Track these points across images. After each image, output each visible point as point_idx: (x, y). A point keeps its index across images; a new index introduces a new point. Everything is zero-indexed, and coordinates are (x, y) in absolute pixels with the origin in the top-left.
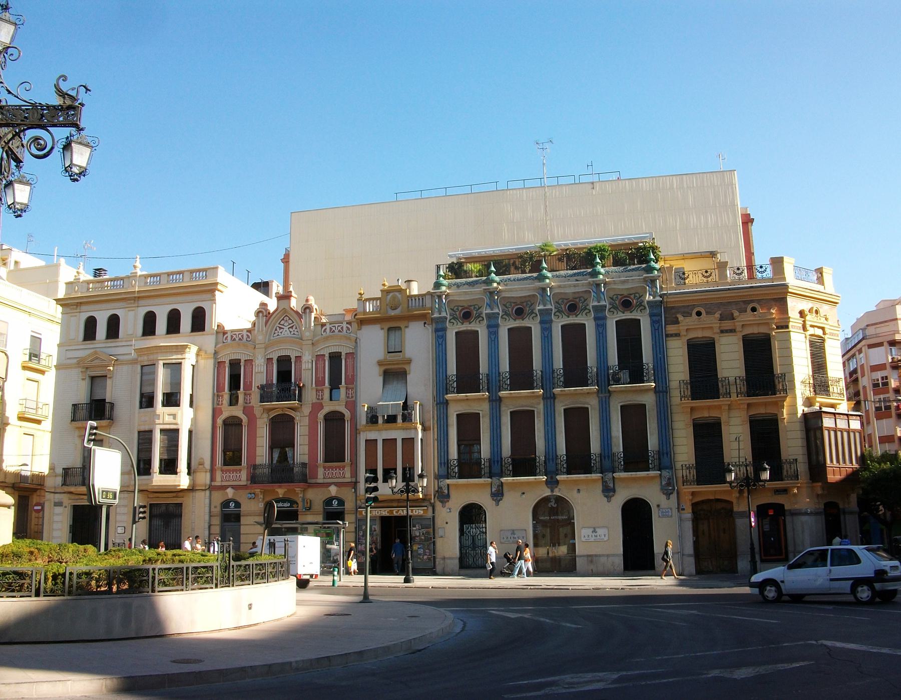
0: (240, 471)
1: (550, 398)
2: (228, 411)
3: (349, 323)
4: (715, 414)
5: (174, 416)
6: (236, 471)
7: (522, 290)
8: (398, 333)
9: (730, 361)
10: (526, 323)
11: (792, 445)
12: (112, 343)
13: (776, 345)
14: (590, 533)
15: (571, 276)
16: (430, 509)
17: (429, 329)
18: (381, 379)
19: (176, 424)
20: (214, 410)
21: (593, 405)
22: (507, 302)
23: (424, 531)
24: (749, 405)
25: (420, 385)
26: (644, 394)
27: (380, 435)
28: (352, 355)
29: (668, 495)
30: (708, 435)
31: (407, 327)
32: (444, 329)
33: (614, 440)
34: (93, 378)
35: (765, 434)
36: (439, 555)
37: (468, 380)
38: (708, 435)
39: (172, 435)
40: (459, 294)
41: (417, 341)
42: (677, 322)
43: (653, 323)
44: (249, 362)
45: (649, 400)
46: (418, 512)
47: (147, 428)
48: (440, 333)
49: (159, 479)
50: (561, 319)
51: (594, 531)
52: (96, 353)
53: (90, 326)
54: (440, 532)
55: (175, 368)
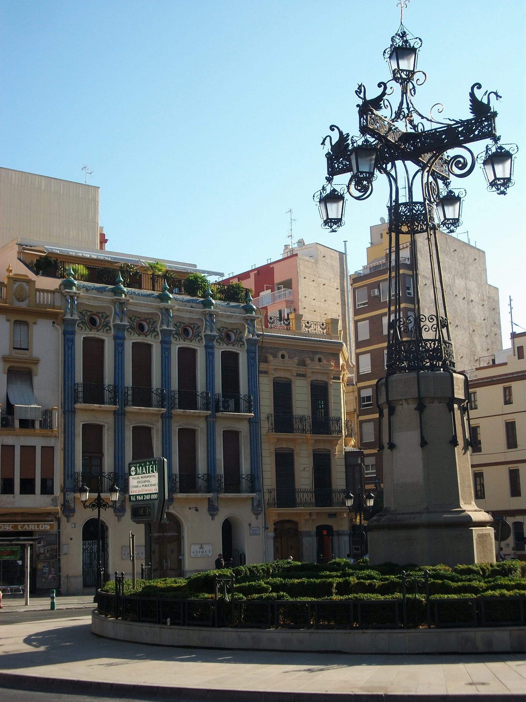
1: (167, 418)
4: (291, 446)
7: (146, 306)
8: (24, 328)
9: (302, 403)
10: (148, 340)
11: (339, 478)
13: (332, 392)
14: (198, 550)
15: (189, 301)
16: (55, 523)
17: (60, 330)
18: (5, 376)
21: (201, 427)
22: (133, 316)
23: (49, 548)
24: (316, 441)
26: (238, 421)
27: (18, 440)
29: (257, 514)
30: (285, 461)
31: (35, 323)
32: (73, 333)
33: (217, 462)
36: (63, 574)
37: (93, 392)
38: (285, 461)
40: (89, 298)
41: (45, 340)
42: (266, 361)
45: (244, 428)
46: (45, 527)
48: (69, 336)
50: (221, 347)
51: (201, 548)
54: (64, 549)
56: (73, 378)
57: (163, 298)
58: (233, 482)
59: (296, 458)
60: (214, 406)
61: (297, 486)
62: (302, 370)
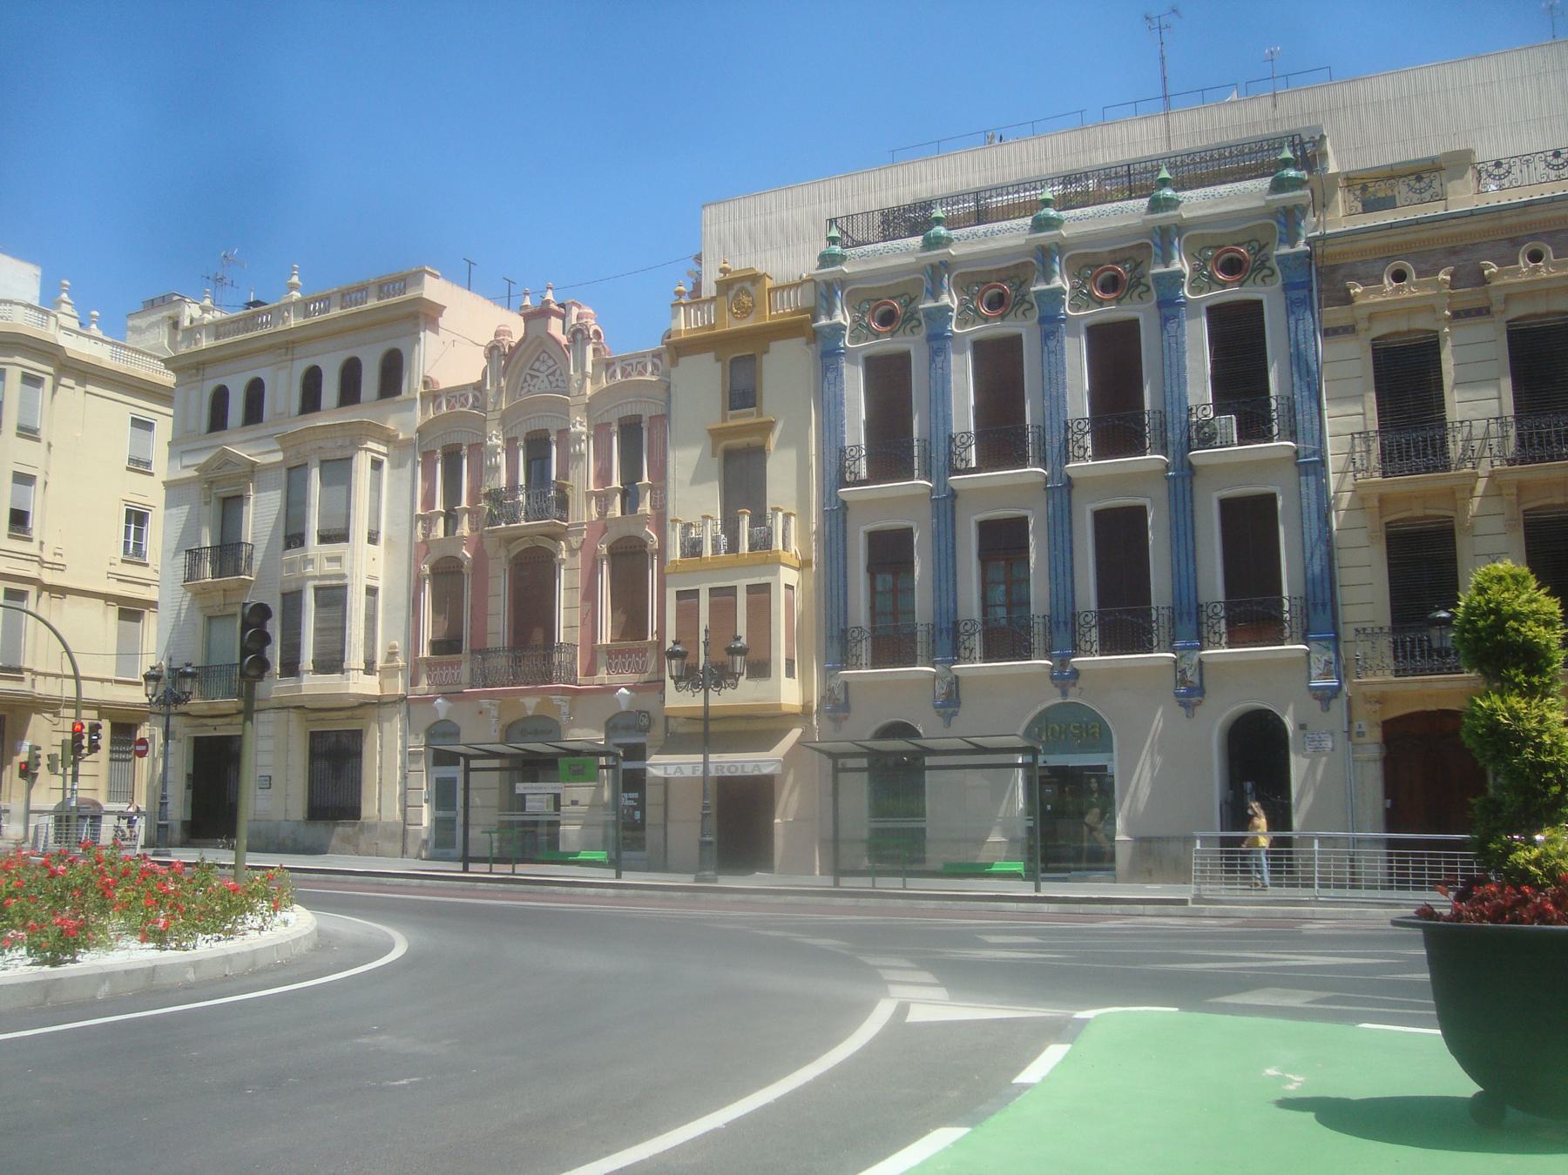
0: (459, 663)
6: (451, 664)
19: (343, 576)
47: (293, 587)
53: (220, 398)
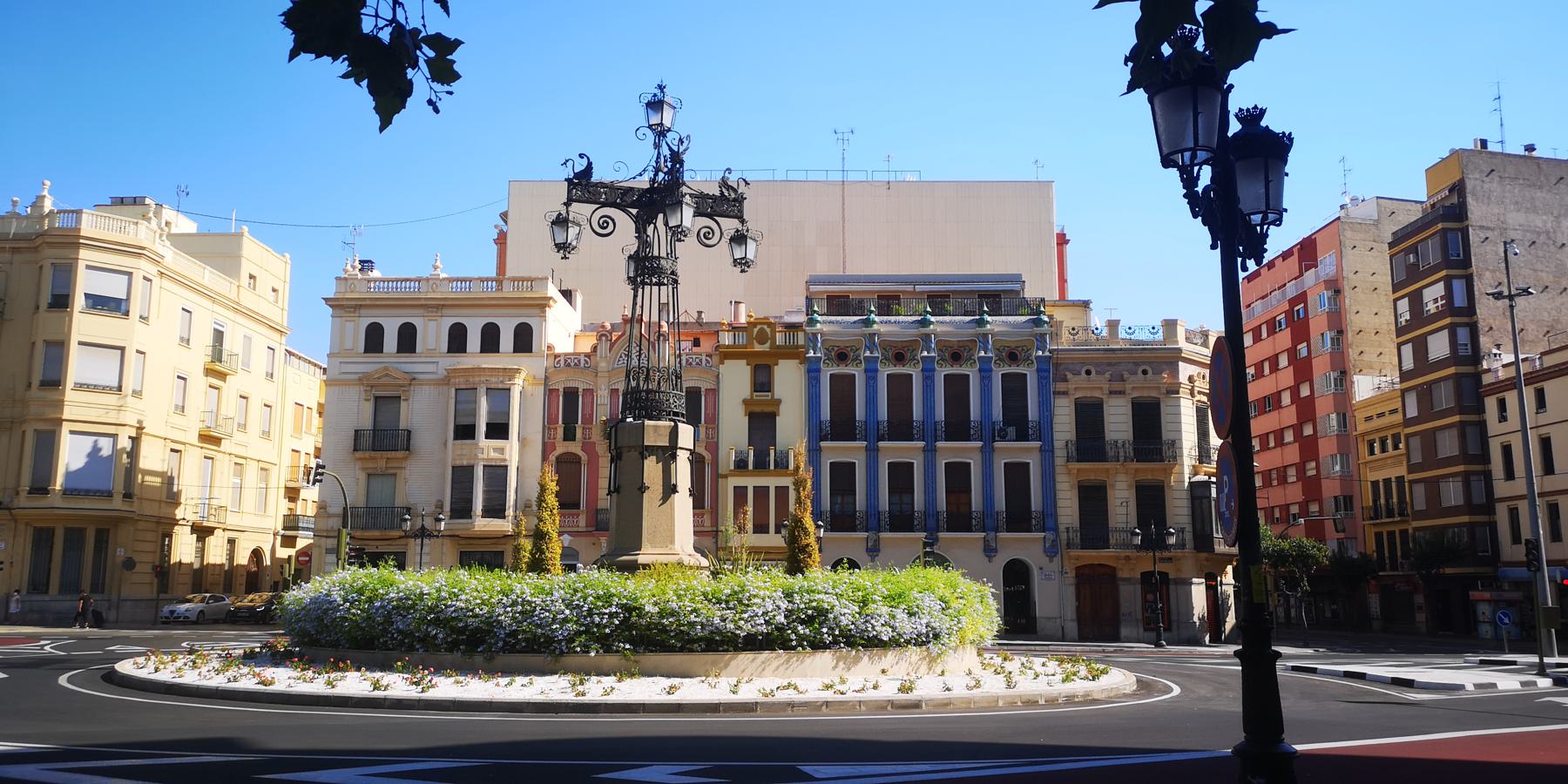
1: (930, 452)
2: (562, 448)
3: (710, 356)
5: (502, 451)
9: (1118, 423)
11: (1178, 511)
12: (404, 358)
17: (803, 368)
20: (544, 444)
22: (886, 345)
25: (791, 430)
28: (714, 392)
29: (1051, 559)
30: (1093, 498)
32: (819, 371)
34: (377, 398)
35: (1151, 499)
37: (842, 427)
38: (1093, 498)
39: (497, 474)
41: (789, 380)
42: (1065, 380)
43: (1040, 379)
44: (589, 392)
49: (482, 524)
52: (386, 369)
55: (501, 395)
56: (876, 412)
57: (924, 323)
58: (1019, 518)
59: (1109, 492)
60: (990, 435)
61: (1111, 524)
62: (1117, 386)
